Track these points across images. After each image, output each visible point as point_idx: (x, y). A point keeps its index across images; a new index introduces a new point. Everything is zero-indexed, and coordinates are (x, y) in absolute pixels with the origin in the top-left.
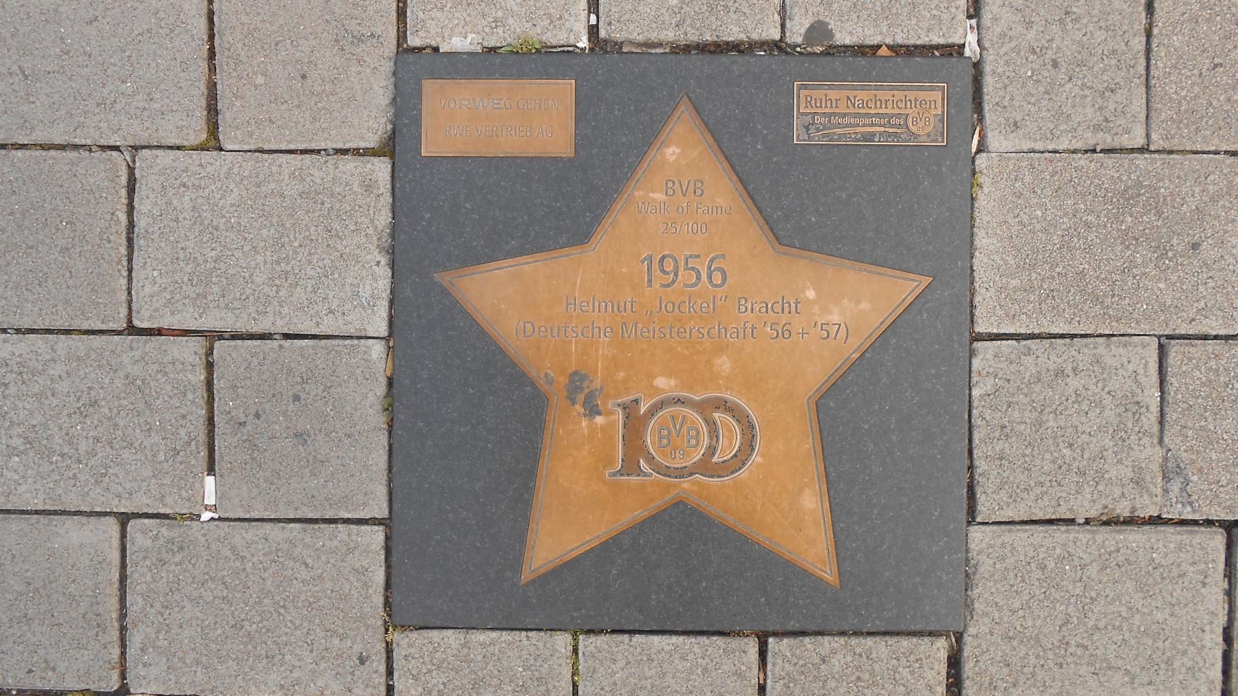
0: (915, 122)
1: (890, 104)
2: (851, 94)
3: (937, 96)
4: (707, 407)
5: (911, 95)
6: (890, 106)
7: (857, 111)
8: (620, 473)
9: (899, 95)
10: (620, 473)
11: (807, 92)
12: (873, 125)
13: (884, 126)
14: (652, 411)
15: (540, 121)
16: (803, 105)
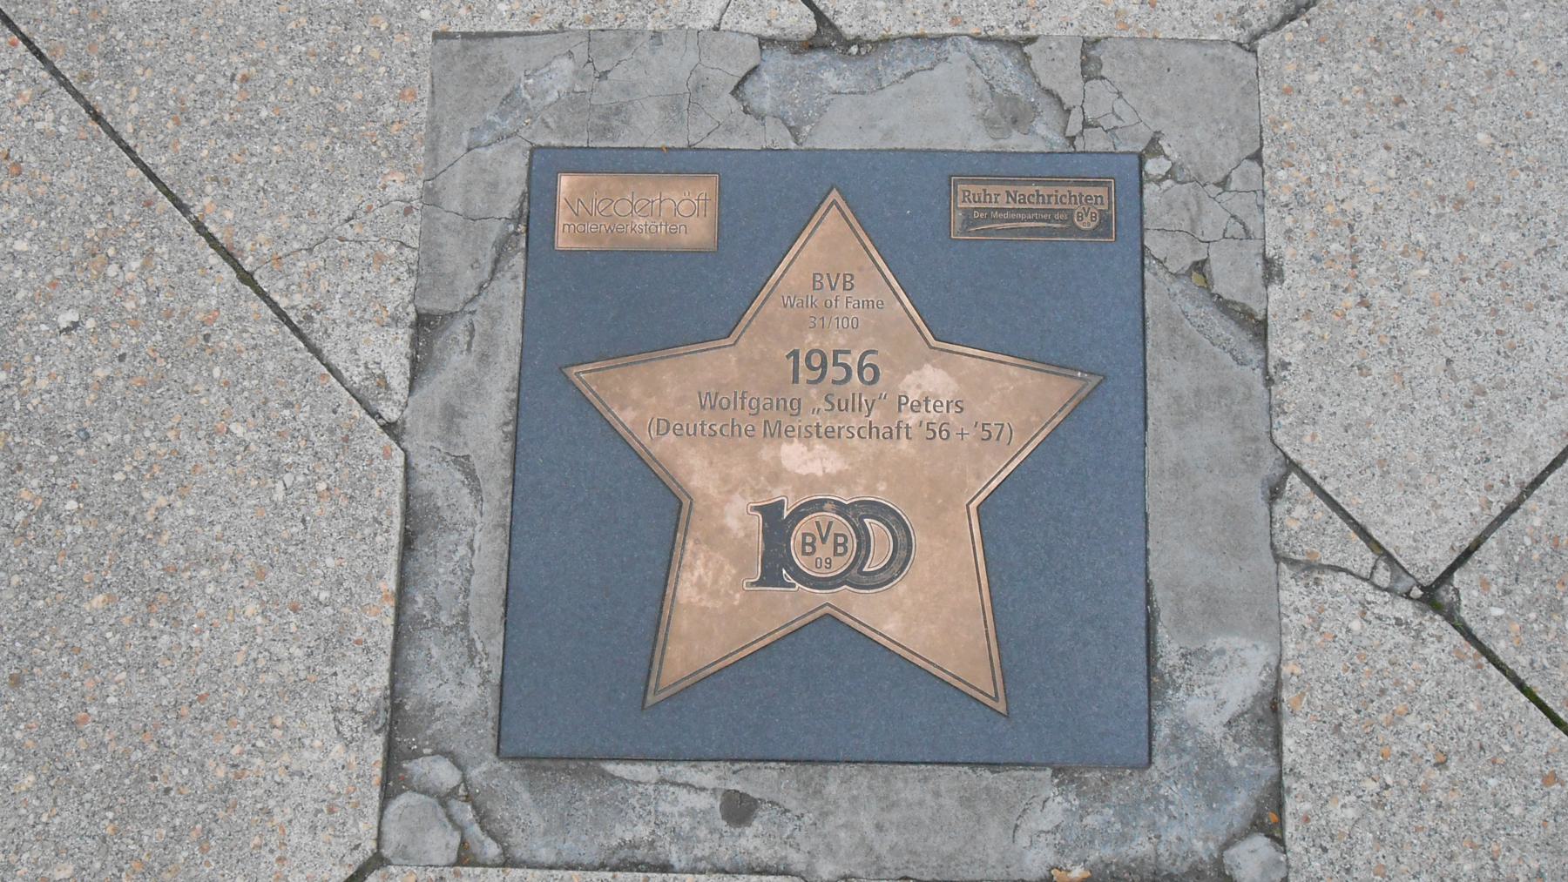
0: (1080, 218)
1: (1053, 199)
2: (1011, 189)
3: (1101, 191)
4: (857, 512)
5: (1075, 190)
6: (1053, 199)
7: (1017, 206)
8: (757, 584)
9: (1063, 190)
10: (757, 584)
11: (965, 187)
12: (1034, 220)
13: (1048, 221)
14: (798, 514)
15: (681, 214)
16: (960, 197)
